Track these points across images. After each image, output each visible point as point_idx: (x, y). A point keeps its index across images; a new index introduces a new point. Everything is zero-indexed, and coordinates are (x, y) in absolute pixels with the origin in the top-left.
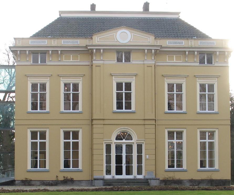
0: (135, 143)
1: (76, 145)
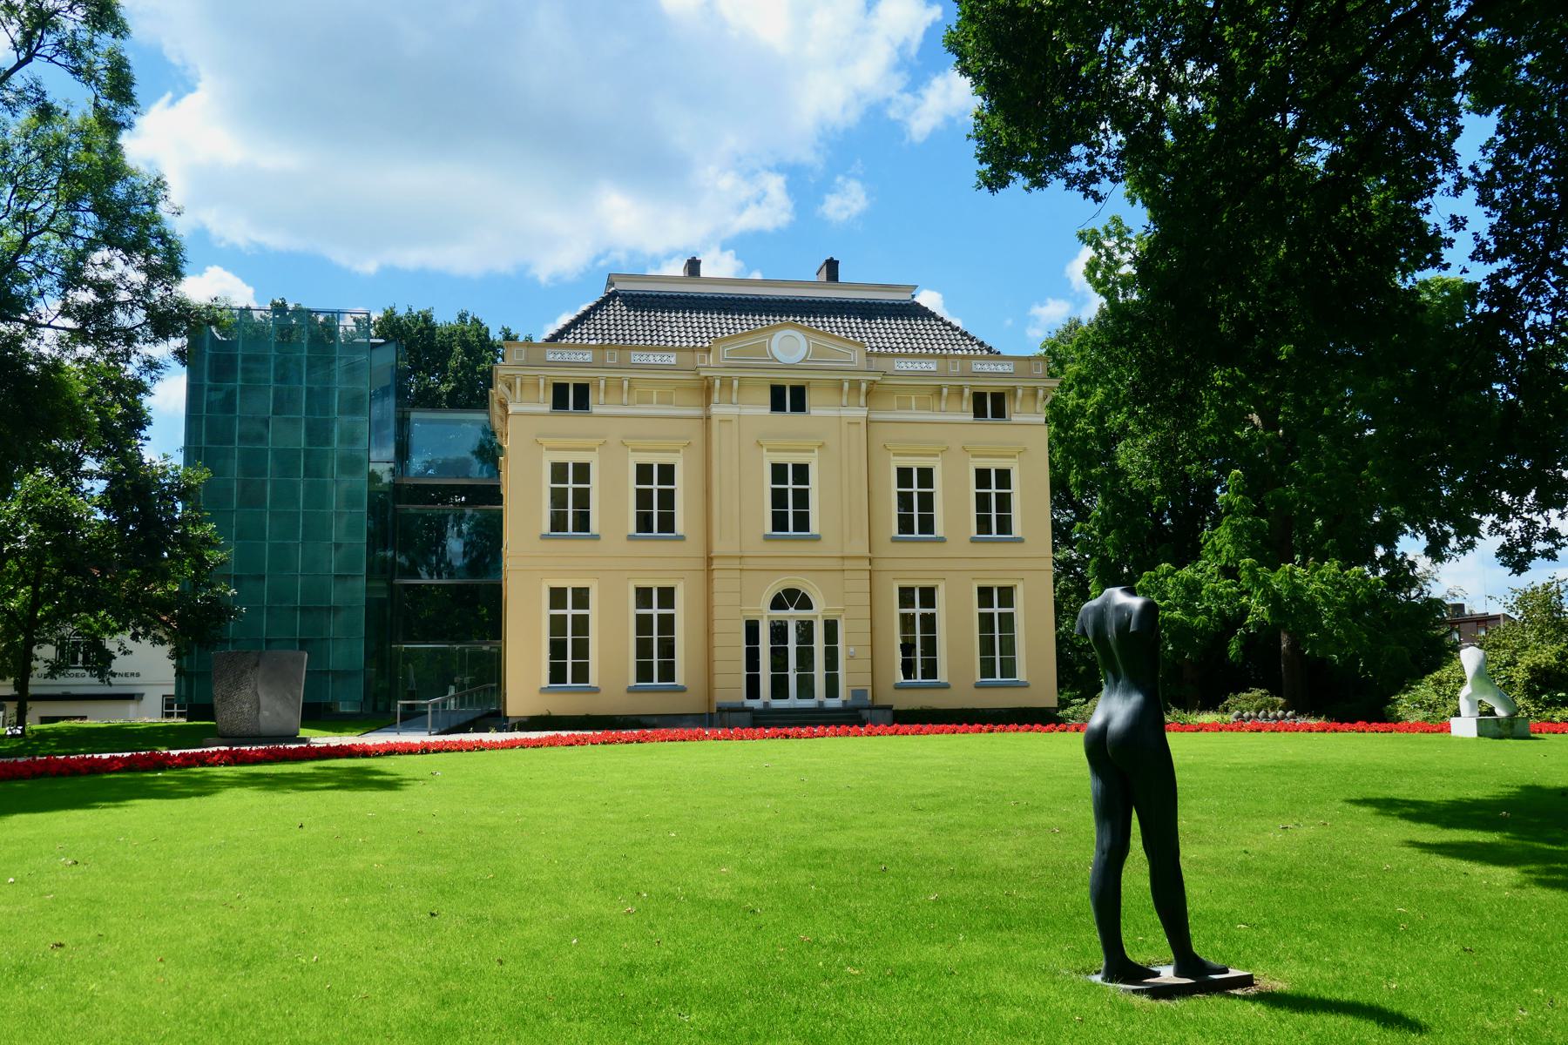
0: (820, 617)
1: (667, 623)
